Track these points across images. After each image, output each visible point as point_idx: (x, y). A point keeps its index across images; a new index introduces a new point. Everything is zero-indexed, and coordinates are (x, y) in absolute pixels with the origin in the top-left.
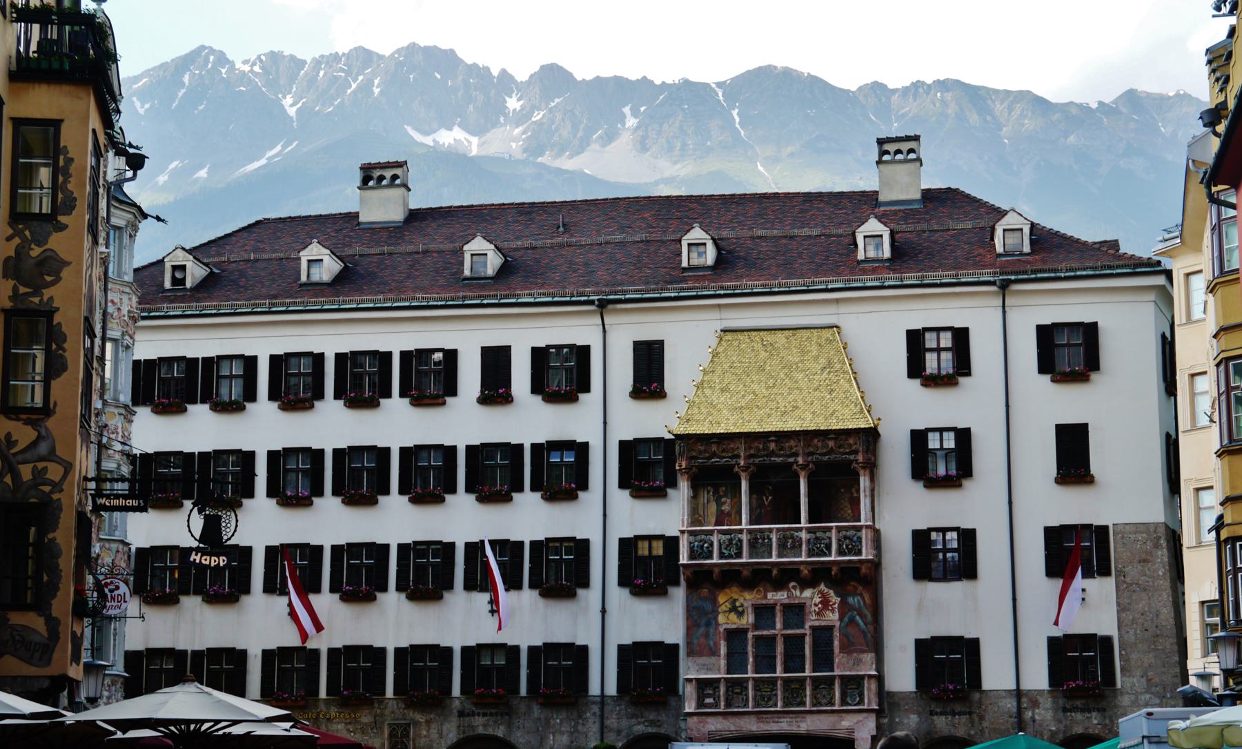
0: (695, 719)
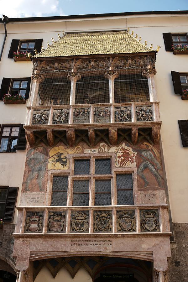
0: (21, 240)
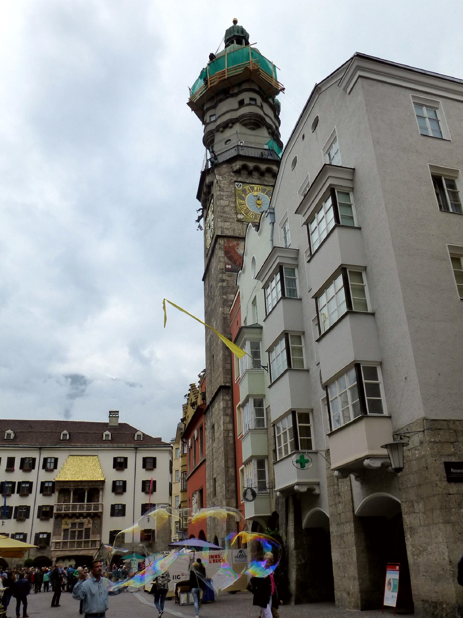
0: (53, 552)
